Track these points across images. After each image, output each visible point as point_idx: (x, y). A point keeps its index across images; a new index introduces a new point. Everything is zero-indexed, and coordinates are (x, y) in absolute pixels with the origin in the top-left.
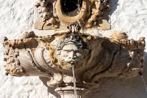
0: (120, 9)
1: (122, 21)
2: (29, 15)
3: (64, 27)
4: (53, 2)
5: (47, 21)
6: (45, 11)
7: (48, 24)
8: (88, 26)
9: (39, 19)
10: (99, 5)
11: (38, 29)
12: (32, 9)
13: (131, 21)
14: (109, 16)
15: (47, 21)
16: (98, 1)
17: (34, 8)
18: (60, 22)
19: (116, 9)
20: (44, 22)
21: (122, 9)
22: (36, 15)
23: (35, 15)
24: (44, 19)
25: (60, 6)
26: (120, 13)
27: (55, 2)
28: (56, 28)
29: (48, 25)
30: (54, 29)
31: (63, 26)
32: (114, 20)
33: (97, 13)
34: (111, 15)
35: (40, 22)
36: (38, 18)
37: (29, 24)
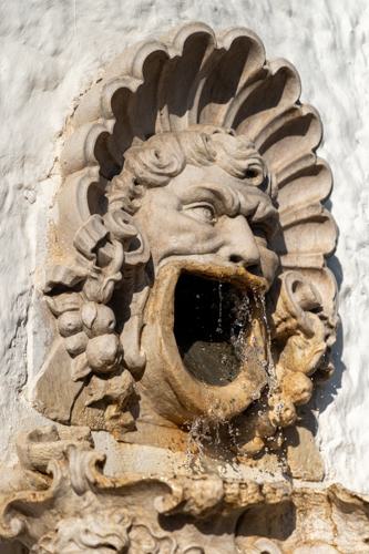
0: (354, 391)
1: (358, 451)
2: (11, 330)
3: (152, 426)
4: (139, 289)
5: (95, 379)
6: (112, 326)
7: (98, 396)
8: (255, 444)
9: (58, 360)
10: (318, 356)
11: (53, 416)
12: (21, 295)
13: (114, 423)
14: (316, 413)
15: (95, 379)
16: (309, 334)
17: (30, 295)
18: (139, 398)
19: (340, 386)
20: (81, 383)
21: (357, 394)
22: (38, 336)
23: (35, 333)
24: (83, 369)
25: (172, 320)
26: (350, 409)
27: (146, 288)
28: (124, 426)
29: (93, 405)
30: (111, 432)
31: (147, 422)
32: (332, 439)
33: (304, 391)
34: (321, 412)
35: (63, 378)
36: (50, 357)
37: (9, 377)
